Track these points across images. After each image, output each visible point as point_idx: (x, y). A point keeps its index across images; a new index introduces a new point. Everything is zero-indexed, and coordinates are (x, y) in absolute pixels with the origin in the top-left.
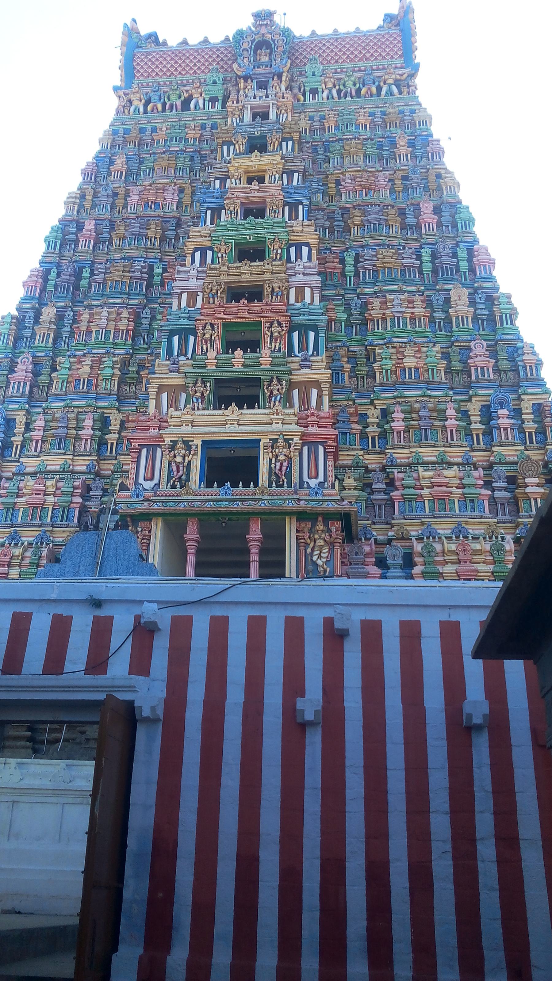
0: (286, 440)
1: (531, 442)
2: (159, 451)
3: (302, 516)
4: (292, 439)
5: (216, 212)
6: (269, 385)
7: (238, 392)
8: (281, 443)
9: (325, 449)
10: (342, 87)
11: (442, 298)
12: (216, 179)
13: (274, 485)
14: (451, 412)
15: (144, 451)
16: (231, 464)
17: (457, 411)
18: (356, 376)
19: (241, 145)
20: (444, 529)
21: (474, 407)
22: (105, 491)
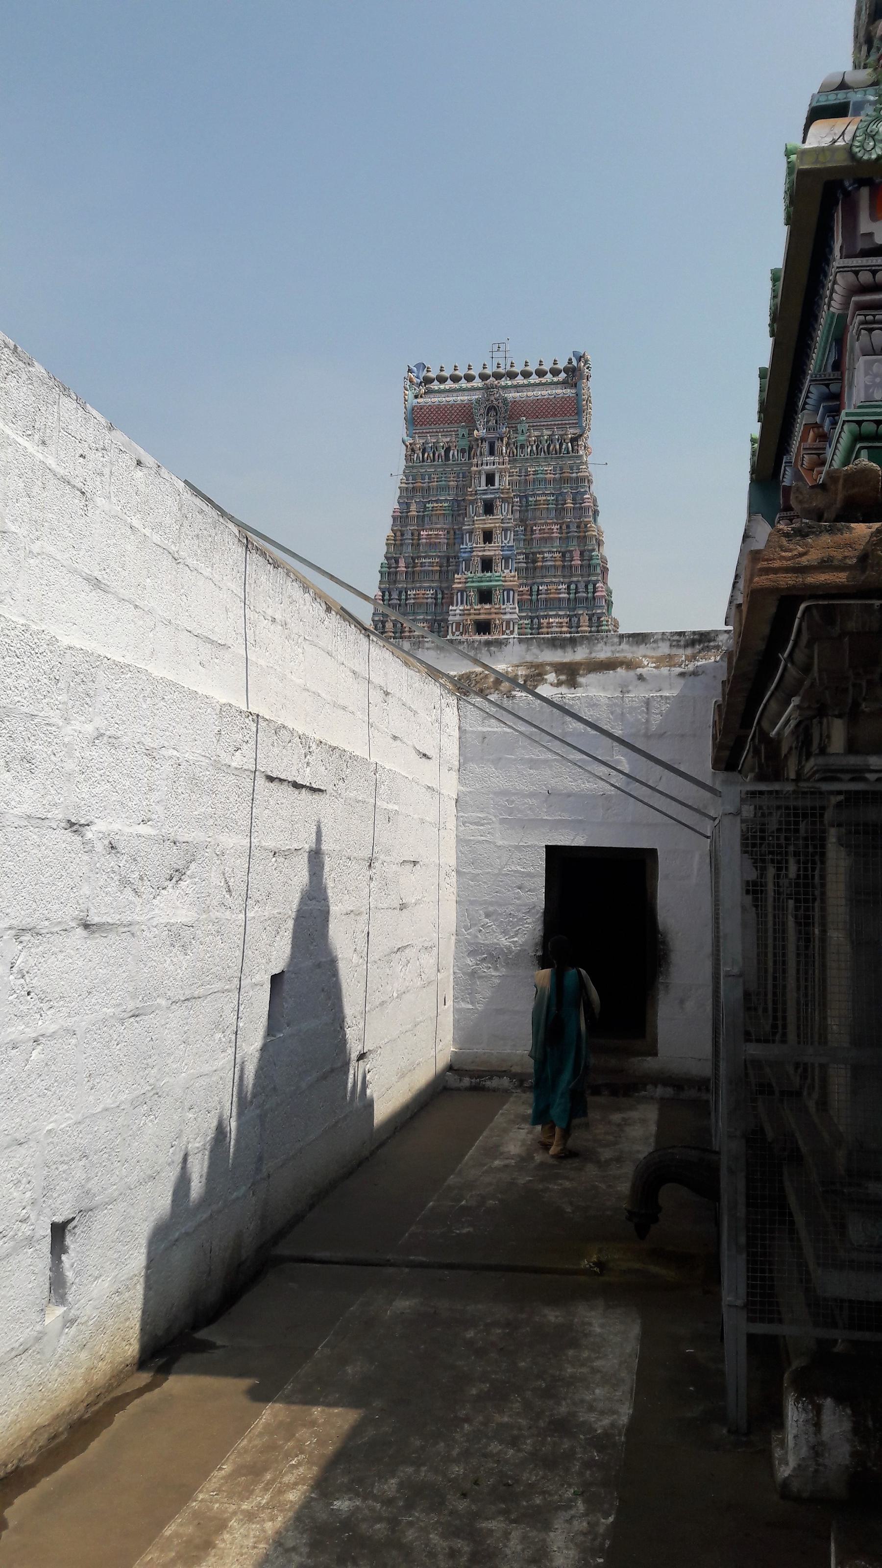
11: (576, 620)
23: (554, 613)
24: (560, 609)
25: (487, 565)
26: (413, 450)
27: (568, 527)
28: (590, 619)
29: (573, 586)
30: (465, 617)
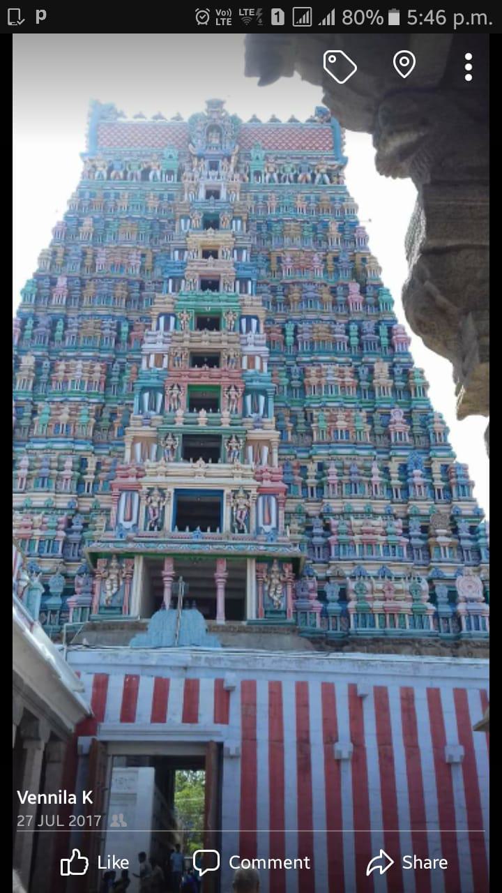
0: (245, 492)
1: (440, 498)
2: (136, 496)
3: (260, 559)
4: (250, 491)
5: (177, 280)
6: (229, 442)
7: (202, 448)
8: (241, 494)
9: (277, 499)
10: (282, 172)
11: (366, 370)
12: (176, 249)
13: (236, 531)
14: (375, 470)
15: (124, 495)
16: (198, 511)
17: (381, 469)
18: (297, 433)
19: (197, 221)
20: (372, 570)
21: (394, 466)
22: (85, 525)
23: (327, 358)
24: (337, 354)
25: (210, 284)
26: (94, 167)
27: (336, 259)
28: (392, 373)
29: (354, 327)
30: (175, 344)
